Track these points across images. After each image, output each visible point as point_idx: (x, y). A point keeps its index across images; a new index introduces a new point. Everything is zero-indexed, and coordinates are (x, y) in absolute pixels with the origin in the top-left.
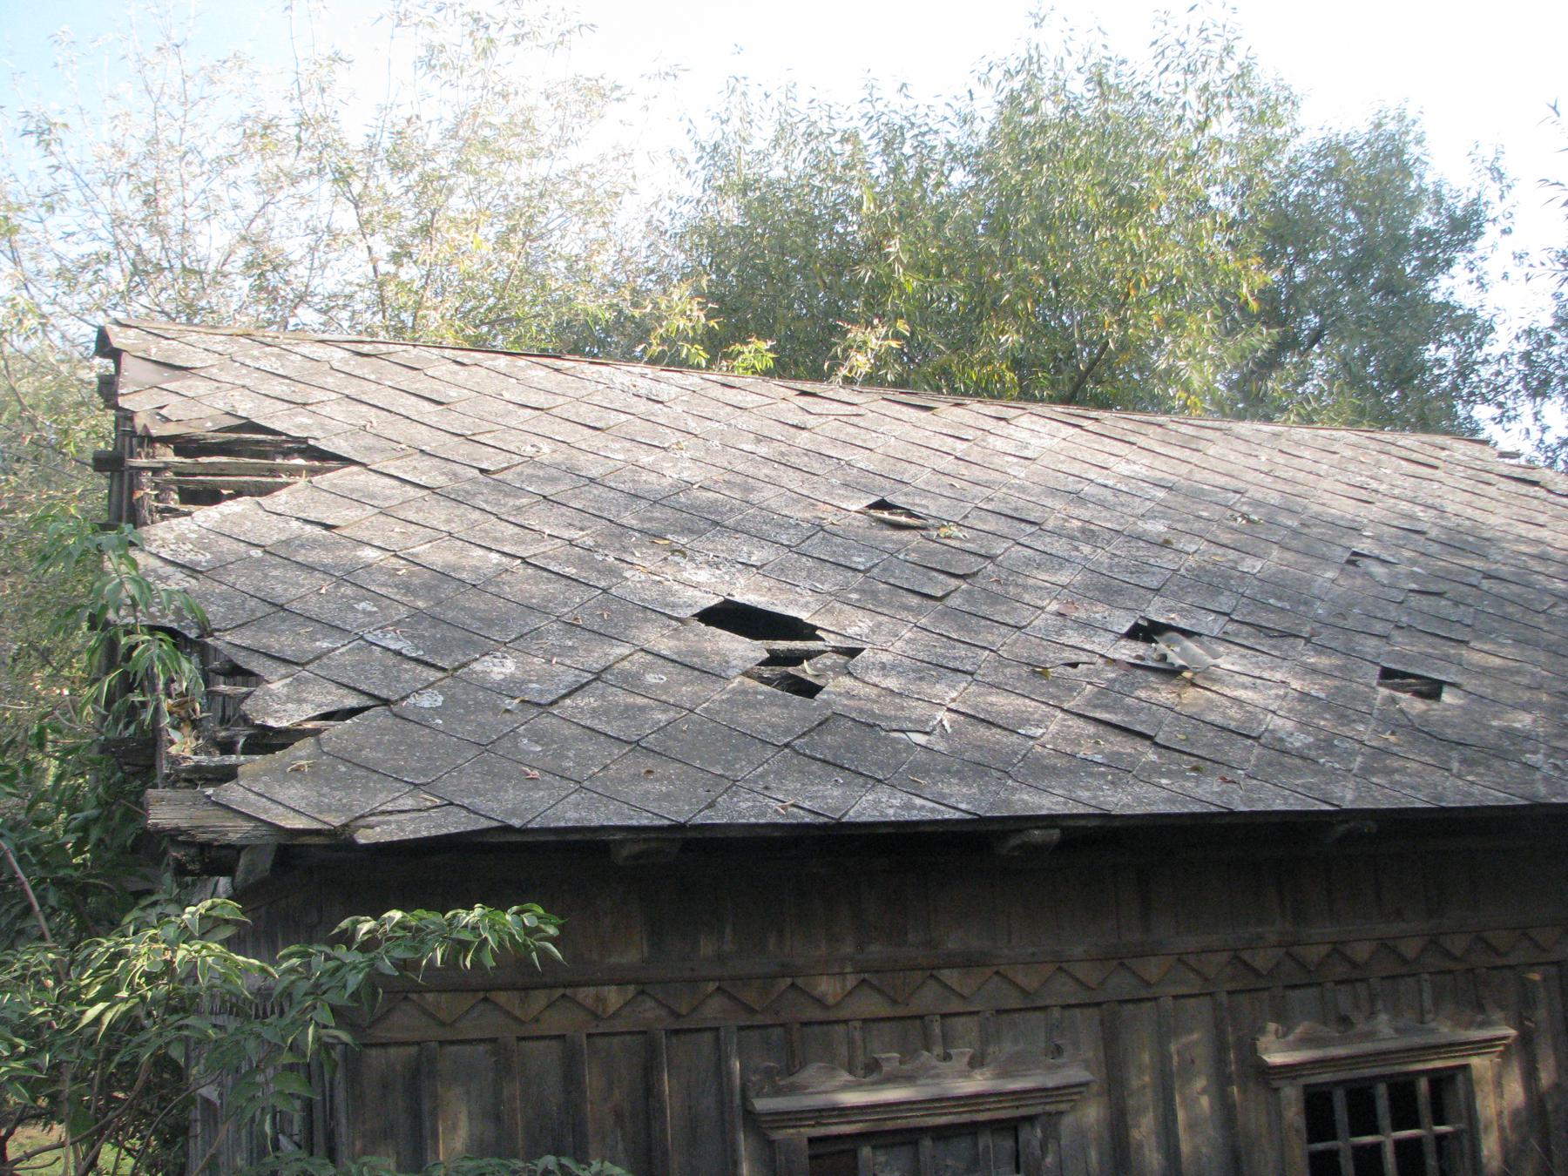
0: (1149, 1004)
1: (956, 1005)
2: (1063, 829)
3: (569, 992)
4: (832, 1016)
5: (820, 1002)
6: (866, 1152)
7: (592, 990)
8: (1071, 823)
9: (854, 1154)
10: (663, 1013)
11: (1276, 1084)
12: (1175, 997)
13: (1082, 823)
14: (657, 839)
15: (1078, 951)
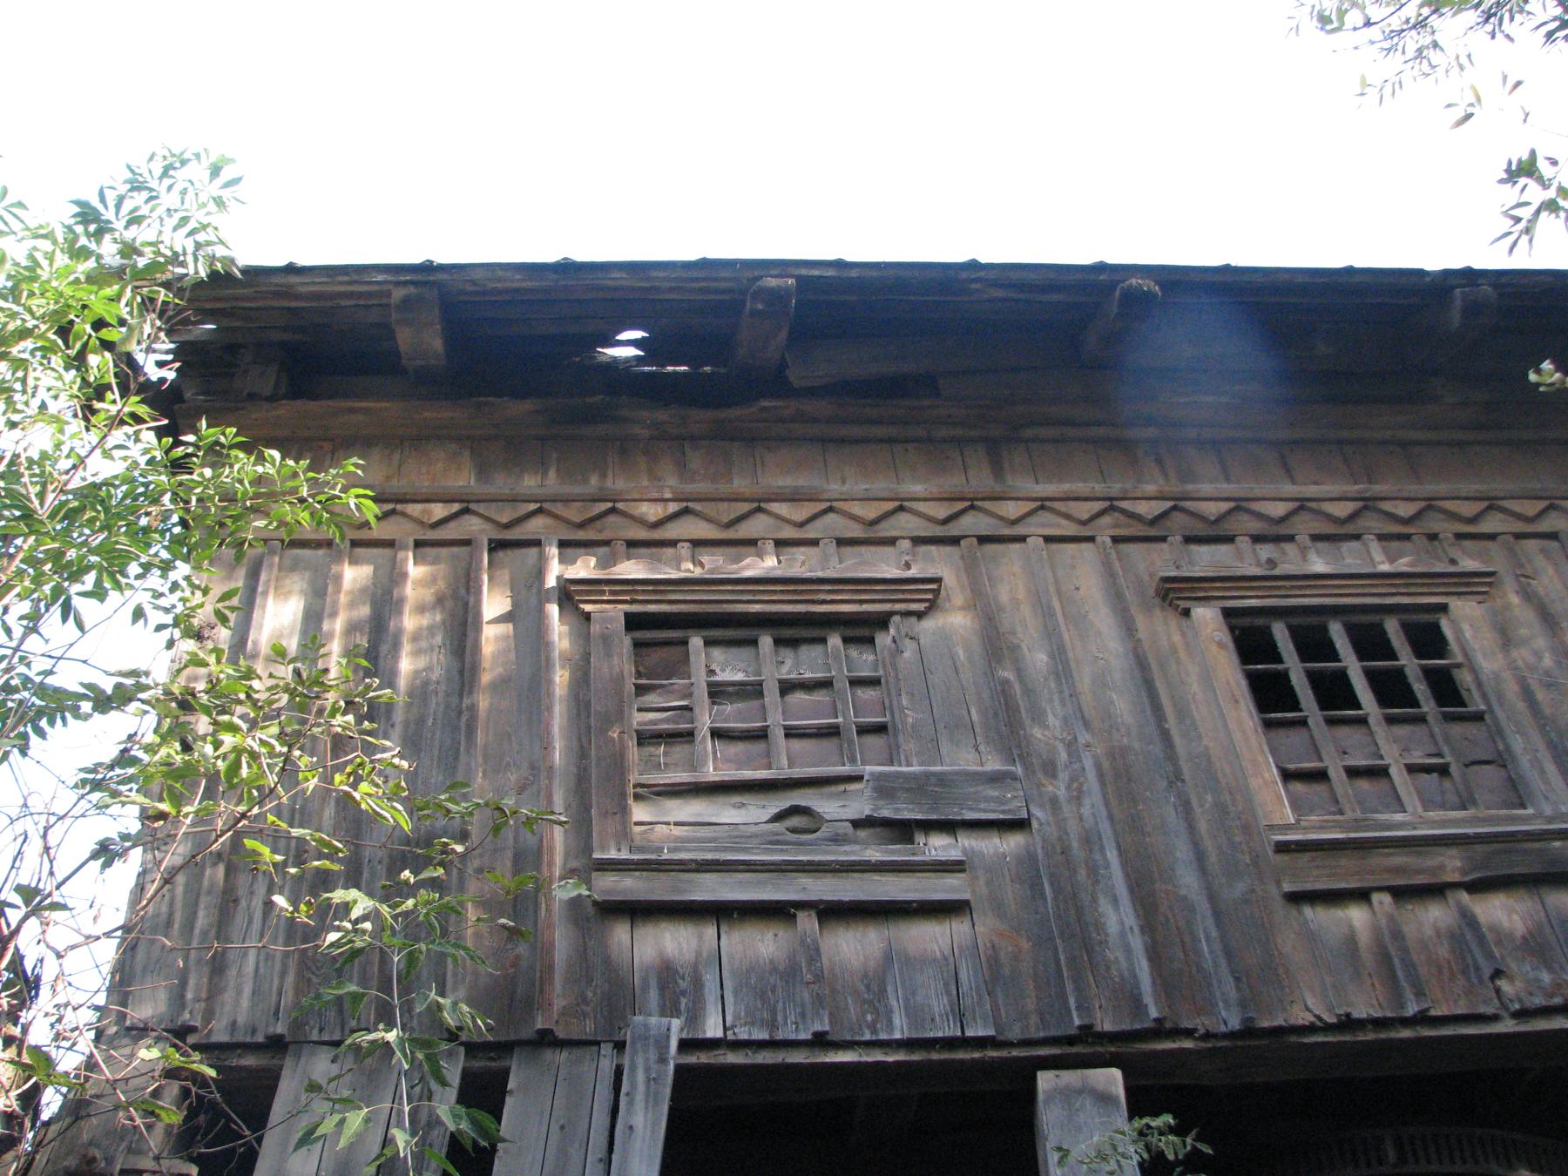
0: (1017, 546)
1: (789, 533)
2: (799, 278)
3: (399, 507)
4: (657, 535)
5: (641, 521)
6: (696, 642)
7: (419, 507)
8: (804, 272)
9: (685, 643)
10: (488, 526)
11: (1183, 604)
12: (1048, 539)
13: (816, 273)
14: (412, 283)
15: (918, 489)
